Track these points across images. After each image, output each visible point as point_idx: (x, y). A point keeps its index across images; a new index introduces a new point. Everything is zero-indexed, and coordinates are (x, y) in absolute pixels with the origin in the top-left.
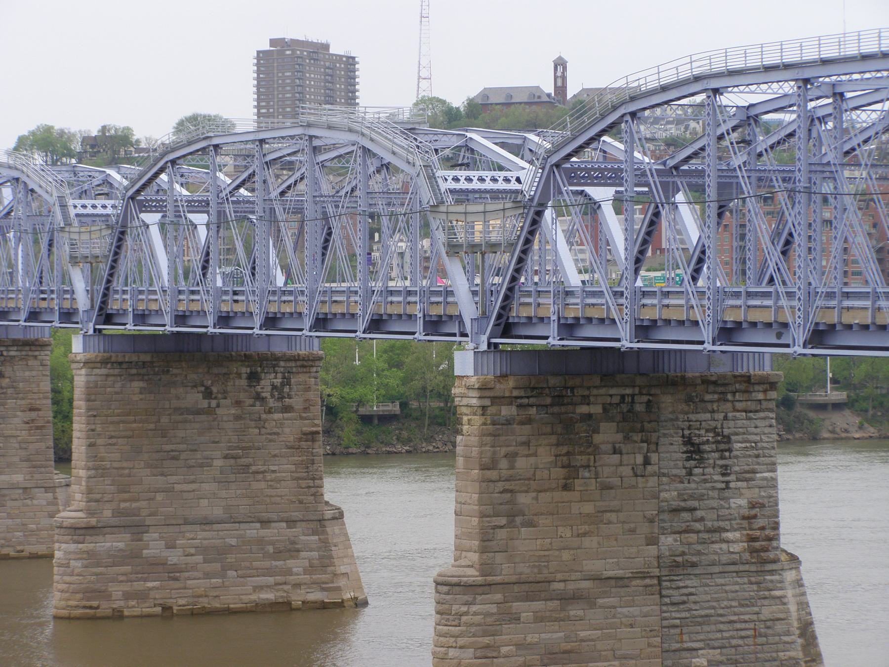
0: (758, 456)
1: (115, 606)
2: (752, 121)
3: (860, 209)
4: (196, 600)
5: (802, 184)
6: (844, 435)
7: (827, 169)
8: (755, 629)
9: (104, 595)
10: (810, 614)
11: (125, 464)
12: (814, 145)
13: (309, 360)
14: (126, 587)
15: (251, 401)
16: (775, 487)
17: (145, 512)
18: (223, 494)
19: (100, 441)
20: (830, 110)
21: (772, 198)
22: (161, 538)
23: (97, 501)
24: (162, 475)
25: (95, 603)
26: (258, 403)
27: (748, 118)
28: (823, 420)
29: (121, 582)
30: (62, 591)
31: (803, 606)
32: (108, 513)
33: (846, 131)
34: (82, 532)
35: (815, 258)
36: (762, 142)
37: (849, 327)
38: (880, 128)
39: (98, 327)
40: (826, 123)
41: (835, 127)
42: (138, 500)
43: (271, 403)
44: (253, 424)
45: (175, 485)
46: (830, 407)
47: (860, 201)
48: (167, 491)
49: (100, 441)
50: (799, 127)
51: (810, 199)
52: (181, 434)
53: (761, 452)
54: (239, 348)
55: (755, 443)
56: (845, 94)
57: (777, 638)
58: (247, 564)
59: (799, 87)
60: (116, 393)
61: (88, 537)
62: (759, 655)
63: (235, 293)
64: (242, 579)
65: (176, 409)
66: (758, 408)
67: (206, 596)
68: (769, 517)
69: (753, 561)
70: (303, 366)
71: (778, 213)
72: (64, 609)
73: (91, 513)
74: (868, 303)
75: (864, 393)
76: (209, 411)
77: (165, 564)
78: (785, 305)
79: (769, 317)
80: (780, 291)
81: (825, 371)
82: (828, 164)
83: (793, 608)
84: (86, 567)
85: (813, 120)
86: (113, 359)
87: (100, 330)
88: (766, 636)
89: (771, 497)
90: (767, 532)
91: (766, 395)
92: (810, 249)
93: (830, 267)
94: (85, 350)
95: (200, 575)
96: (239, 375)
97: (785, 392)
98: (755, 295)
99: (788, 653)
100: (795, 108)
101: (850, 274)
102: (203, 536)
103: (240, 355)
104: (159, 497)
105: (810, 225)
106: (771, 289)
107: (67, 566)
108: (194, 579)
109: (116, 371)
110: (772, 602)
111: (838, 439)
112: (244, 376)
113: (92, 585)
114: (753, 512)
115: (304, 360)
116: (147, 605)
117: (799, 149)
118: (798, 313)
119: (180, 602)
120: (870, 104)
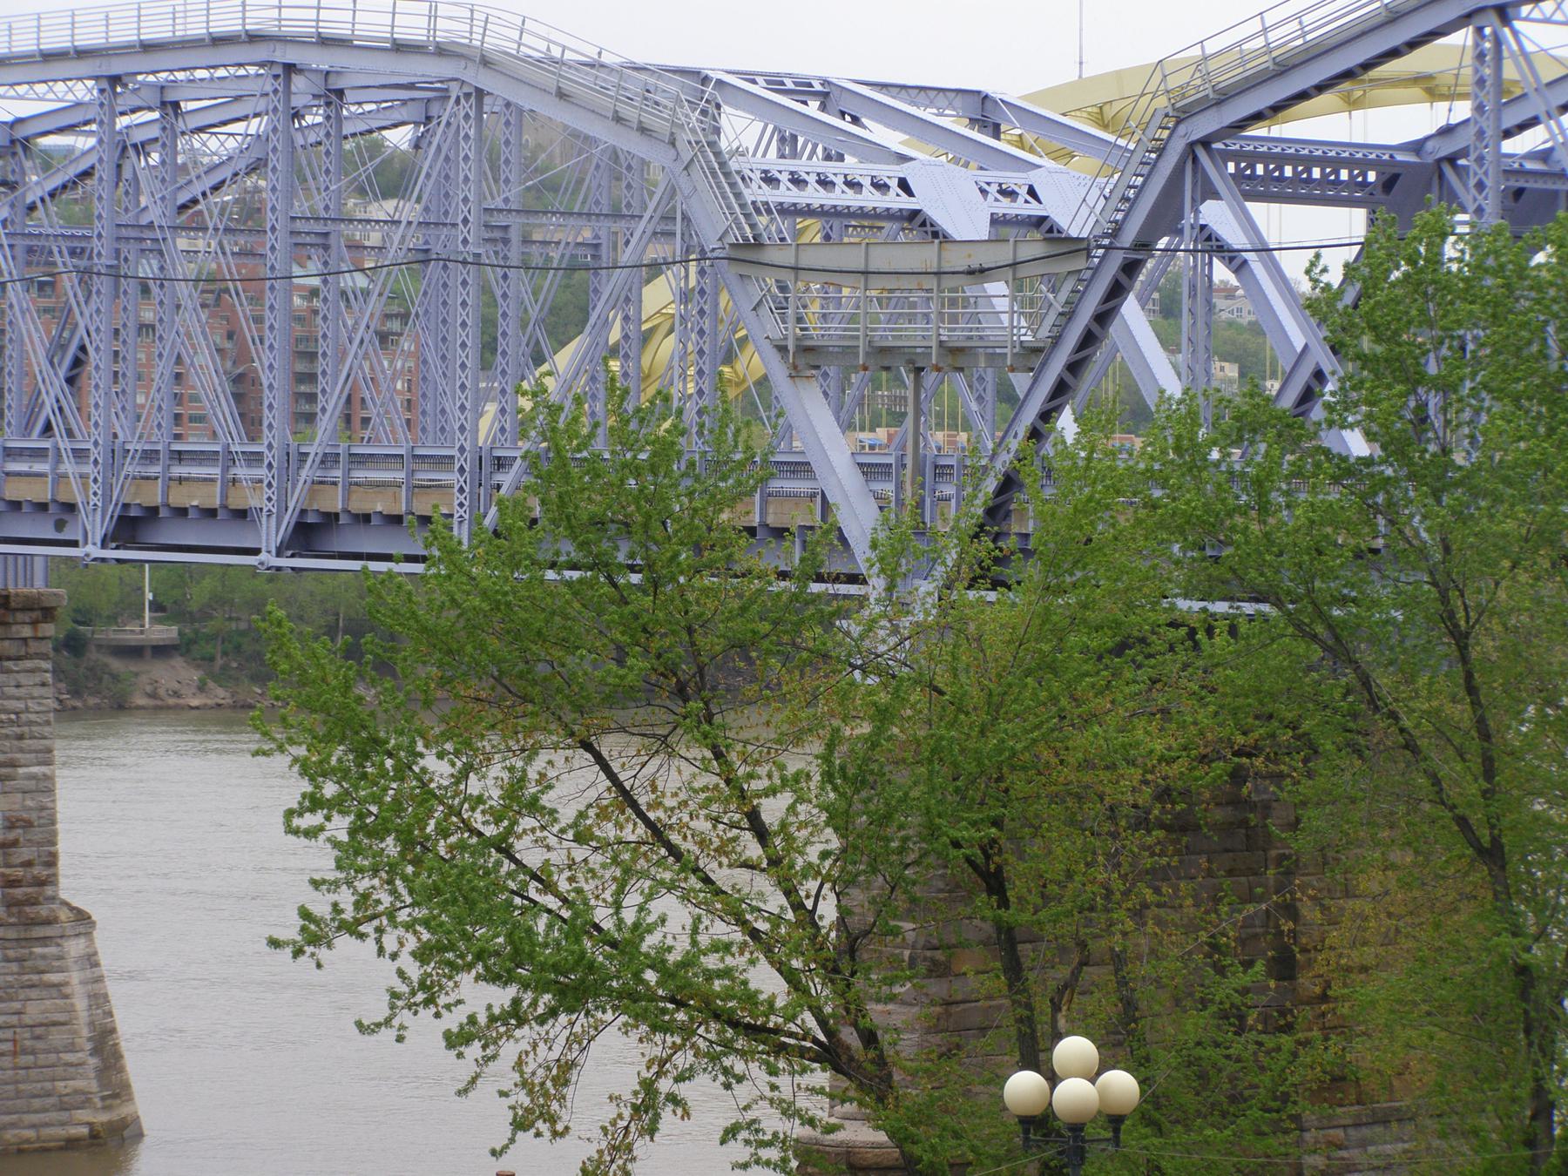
0: (20, 737)
2: (19, 150)
3: (203, 306)
5: (103, 261)
6: (172, 701)
7: (147, 234)
8: (14, 1041)
10: (110, 1014)
12: (127, 193)
16: (50, 791)
20: (155, 132)
21: (52, 284)
27: (13, 142)
28: (136, 675)
31: (99, 1000)
33: (184, 168)
35: (124, 391)
36: (36, 184)
37: (182, 512)
38: (241, 165)
40: (147, 155)
41: (163, 162)
46: (148, 652)
47: (203, 292)
50: (101, 160)
51: (117, 286)
53: (26, 729)
55: (17, 713)
56: (182, 104)
57: (53, 1057)
59: (102, 91)
62: (22, 1087)
66: (23, 653)
68: (40, 844)
69: (12, 920)
71: (62, 311)
74: (215, 471)
75: (208, 628)
78: (70, 472)
79: (41, 492)
80: (62, 446)
81: (141, 589)
82: (150, 226)
83: (80, 1004)
85: (125, 148)
88: (33, 1052)
89: (43, 809)
90: (36, 870)
91: (35, 630)
92: (116, 373)
93: (152, 407)
97: (71, 625)
98: (18, 454)
99: (71, 1083)
100: (94, 127)
101: (185, 419)
105: (117, 331)
106: (46, 444)
110: (44, 993)
111: (160, 708)
114: (12, 835)
117: (100, 198)
118: (93, 487)
120: (225, 123)
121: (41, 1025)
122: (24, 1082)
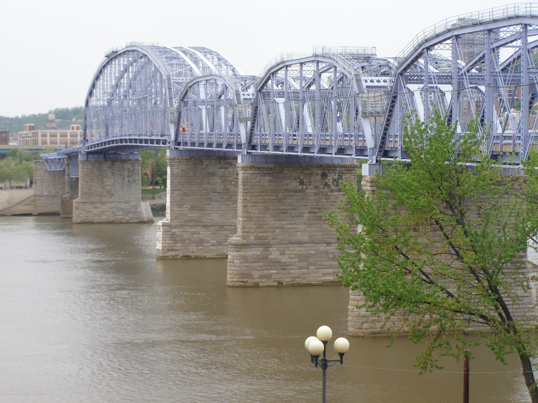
1: (255, 281)
4: (294, 279)
9: (251, 276)
11: (261, 215)
13: (351, 167)
14: (261, 273)
15: (323, 186)
17: (270, 238)
18: (308, 230)
19: (249, 205)
22: (278, 250)
23: (247, 232)
24: (279, 220)
25: (245, 280)
26: (326, 187)
29: (258, 270)
30: (230, 274)
32: (252, 238)
34: (240, 246)
39: (248, 151)
42: (267, 232)
43: (333, 187)
44: (323, 197)
45: (285, 226)
48: (282, 228)
49: (249, 205)
52: (288, 201)
54: (318, 161)
57: (525, 306)
58: (320, 263)
60: (257, 182)
61: (242, 249)
62: (515, 314)
63: (295, 135)
64: (317, 270)
65: (286, 190)
67: (299, 278)
69: (513, 267)
70: (348, 170)
72: (231, 282)
73: (244, 238)
76: (302, 191)
77: (279, 262)
84: (241, 263)
86: (256, 166)
87: (250, 153)
88: (519, 304)
94: (242, 162)
95: (296, 267)
96: (317, 174)
102: (298, 249)
103: (318, 165)
104: (277, 231)
107: (233, 262)
108: (294, 269)
109: (257, 172)
112: (320, 174)
113: (244, 272)
115: (349, 167)
116: (270, 281)
119: (287, 280)
121: (521, 297)
122: (515, 312)
